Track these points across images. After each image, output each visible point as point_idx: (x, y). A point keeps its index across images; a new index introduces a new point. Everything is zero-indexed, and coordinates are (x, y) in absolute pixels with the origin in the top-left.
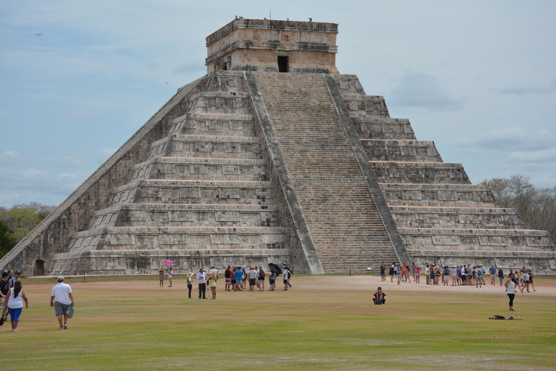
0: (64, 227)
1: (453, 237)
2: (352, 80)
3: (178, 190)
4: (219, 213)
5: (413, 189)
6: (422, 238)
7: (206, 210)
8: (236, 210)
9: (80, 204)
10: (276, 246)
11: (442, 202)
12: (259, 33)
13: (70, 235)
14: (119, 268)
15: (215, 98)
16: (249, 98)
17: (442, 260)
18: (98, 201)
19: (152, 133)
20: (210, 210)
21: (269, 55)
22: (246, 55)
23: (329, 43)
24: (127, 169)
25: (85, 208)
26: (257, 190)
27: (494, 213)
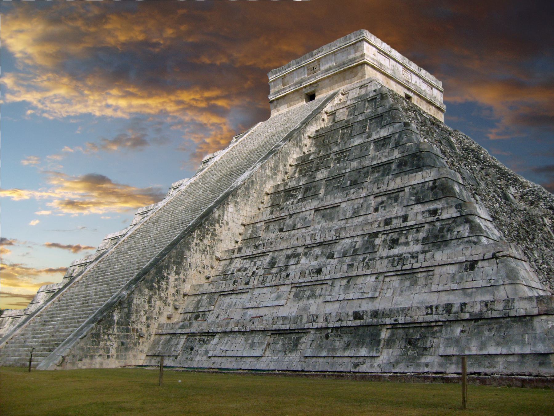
1: (282, 288)
5: (304, 209)
6: (233, 296)
11: (343, 222)
17: (215, 340)
27: (409, 223)
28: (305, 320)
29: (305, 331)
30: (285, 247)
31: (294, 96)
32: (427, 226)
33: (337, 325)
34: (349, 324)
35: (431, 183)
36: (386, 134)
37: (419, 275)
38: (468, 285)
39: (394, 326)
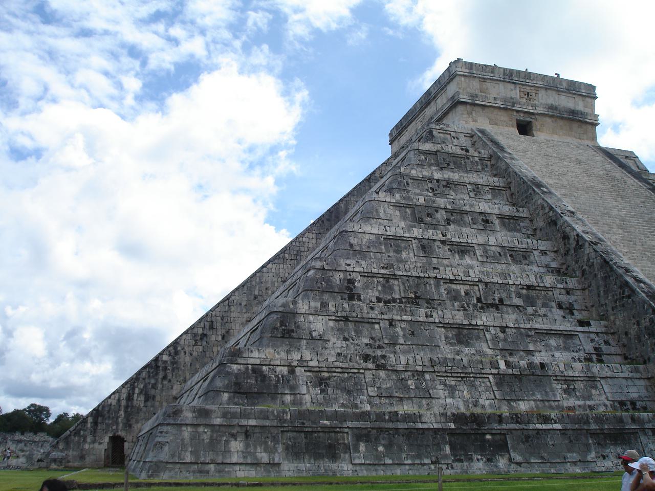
0: (165, 378)
3: (396, 282)
4: (493, 331)
7: (466, 322)
8: (528, 326)
10: (639, 404)
12: (488, 85)
13: (174, 392)
14: (264, 457)
15: (436, 153)
18: (227, 332)
19: (323, 222)
20: (473, 322)
21: (503, 117)
22: (470, 113)
23: (587, 110)
24: (280, 280)
25: (204, 343)
26: (556, 292)
31: (499, 113)
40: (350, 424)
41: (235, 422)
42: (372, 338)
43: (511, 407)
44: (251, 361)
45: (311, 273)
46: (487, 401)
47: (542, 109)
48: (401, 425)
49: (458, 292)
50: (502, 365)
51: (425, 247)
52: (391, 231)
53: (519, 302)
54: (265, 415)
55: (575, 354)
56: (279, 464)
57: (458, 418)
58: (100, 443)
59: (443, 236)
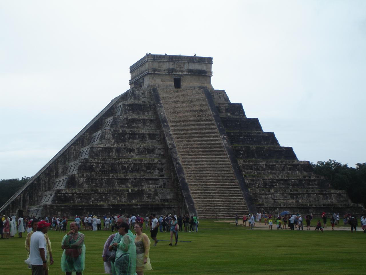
1: (285, 194)
2: (222, 93)
3: (106, 165)
4: (132, 180)
5: (260, 163)
7: (124, 177)
8: (143, 177)
9: (45, 174)
11: (279, 172)
14: (65, 215)
16: (154, 105)
20: (126, 177)
21: (168, 78)
22: (153, 78)
23: (207, 70)
27: (312, 179)
28: (308, 205)
29: (309, 208)
30: (268, 178)
32: (317, 181)
33: (319, 207)
34: (323, 207)
35: (307, 165)
36: (267, 135)
37: (328, 195)
38: (341, 199)
39: (334, 208)
40: (86, 208)
41: (59, 208)
42: (96, 184)
43: (130, 202)
44: (63, 193)
45: (81, 163)
46: (124, 200)
47: (186, 72)
48: (98, 208)
49: (125, 167)
50: (130, 191)
51: (118, 150)
52: (107, 146)
53: (144, 168)
54: (65, 206)
55: (156, 185)
56: (69, 217)
57: (113, 205)
58: (15, 213)
59: (125, 146)
